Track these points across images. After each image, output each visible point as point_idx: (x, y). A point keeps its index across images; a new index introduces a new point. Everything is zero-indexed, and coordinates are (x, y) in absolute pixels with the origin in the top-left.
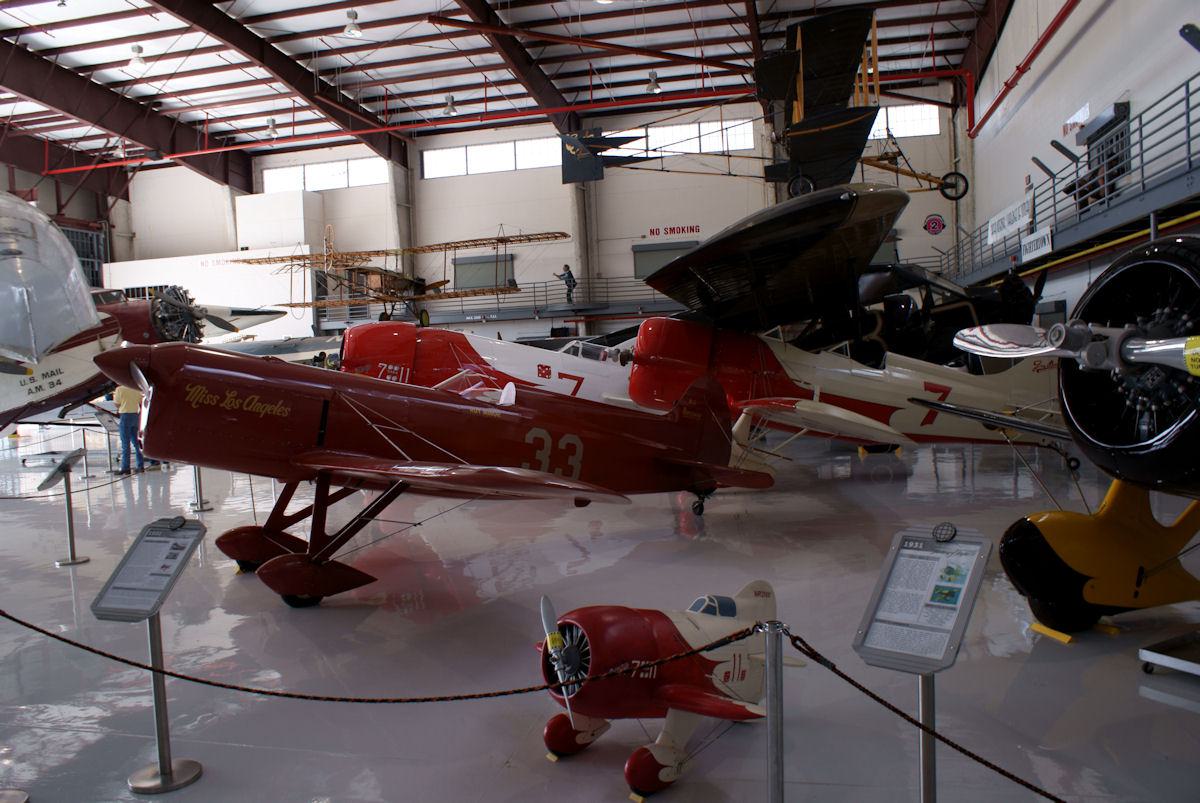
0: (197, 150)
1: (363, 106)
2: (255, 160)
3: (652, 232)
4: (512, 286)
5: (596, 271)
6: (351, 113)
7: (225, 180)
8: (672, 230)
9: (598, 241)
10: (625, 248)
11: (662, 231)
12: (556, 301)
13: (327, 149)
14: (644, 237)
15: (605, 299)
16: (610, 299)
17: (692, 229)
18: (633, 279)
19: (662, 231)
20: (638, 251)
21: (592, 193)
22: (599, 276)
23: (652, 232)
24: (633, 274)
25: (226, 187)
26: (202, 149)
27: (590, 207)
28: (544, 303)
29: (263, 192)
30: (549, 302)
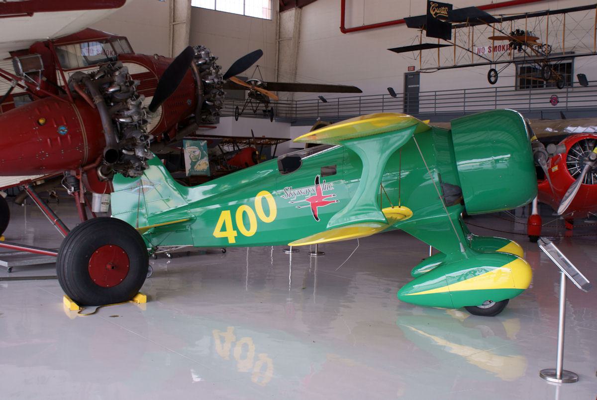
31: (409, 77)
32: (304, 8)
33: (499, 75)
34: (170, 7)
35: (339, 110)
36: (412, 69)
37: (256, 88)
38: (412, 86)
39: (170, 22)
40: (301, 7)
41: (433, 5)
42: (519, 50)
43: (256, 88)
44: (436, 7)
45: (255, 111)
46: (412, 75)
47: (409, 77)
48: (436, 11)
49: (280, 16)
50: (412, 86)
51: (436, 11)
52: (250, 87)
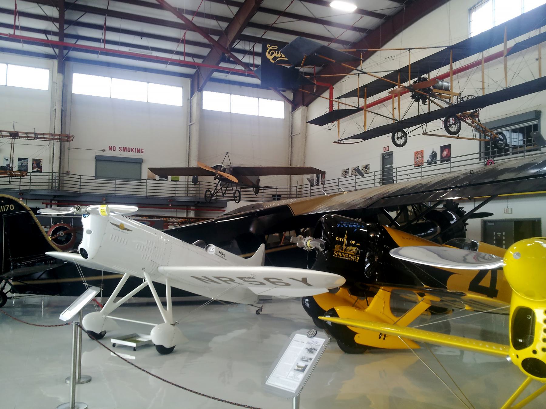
3: (110, 148)
5: (66, 170)
8: (125, 149)
11: (117, 149)
12: (38, 187)
14: (104, 151)
15: (78, 190)
16: (82, 190)
17: (138, 151)
18: (94, 178)
19: (117, 149)
20: (99, 159)
22: (68, 173)
23: (110, 148)
24: (94, 175)
27: (65, 123)
28: (28, 188)
30: (32, 188)
31: (386, 157)
32: (310, 106)
33: (408, 135)
34: (187, 112)
35: (186, 183)
36: (387, 149)
37: (219, 172)
38: (389, 166)
39: (187, 124)
40: (307, 105)
41: (269, 48)
42: (424, 102)
43: (219, 172)
44: (275, 51)
45: (223, 194)
46: (387, 155)
47: (386, 157)
48: (274, 55)
49: (292, 115)
50: (389, 166)
51: (275, 55)
52: (214, 171)
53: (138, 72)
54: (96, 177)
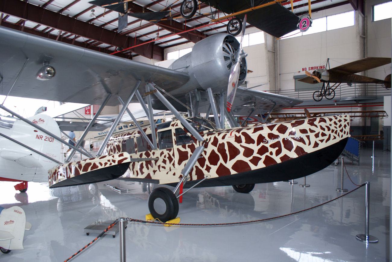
0: (132, 46)
1: (185, 24)
2: (165, 50)
3: (303, 70)
4: (200, 92)
6: (175, 29)
7: (152, 58)
9: (280, 75)
10: (291, 77)
13: (186, 44)
20: (296, 78)
21: (278, 53)
23: (303, 70)
24: (294, 88)
25: (152, 59)
26: (134, 46)
29: (167, 59)
53: (319, 12)
54: (296, 90)
